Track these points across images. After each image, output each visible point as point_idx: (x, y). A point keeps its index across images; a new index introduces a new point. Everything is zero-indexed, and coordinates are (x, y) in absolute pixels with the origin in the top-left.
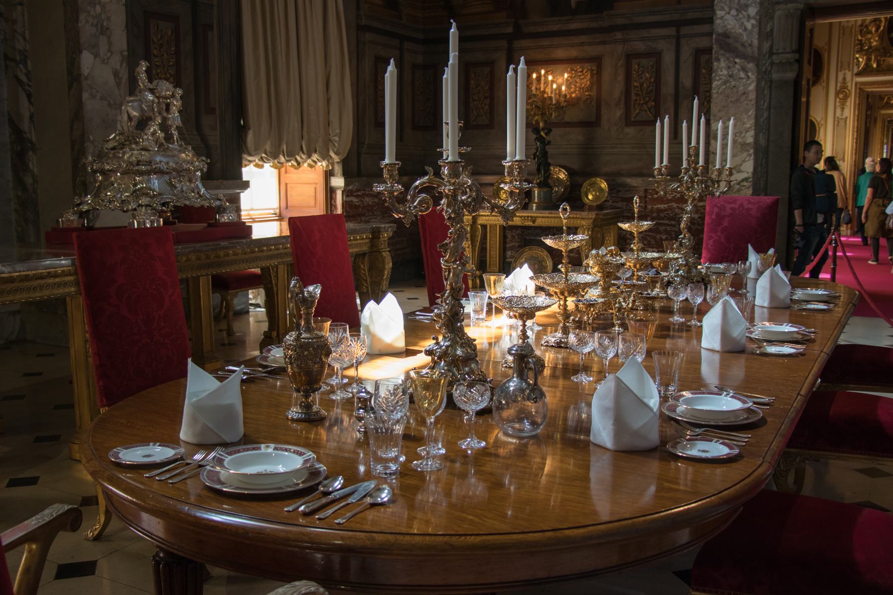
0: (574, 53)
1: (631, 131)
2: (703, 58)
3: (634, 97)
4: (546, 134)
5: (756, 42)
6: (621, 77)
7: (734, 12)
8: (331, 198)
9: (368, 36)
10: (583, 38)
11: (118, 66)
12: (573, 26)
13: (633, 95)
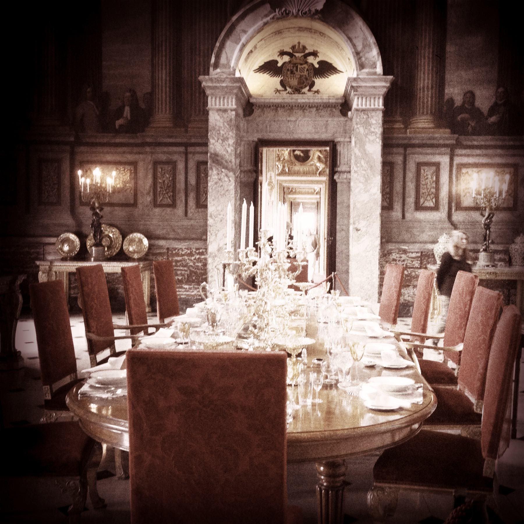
0: (118, 158)
1: (157, 210)
2: (202, 168)
3: (159, 190)
4: (100, 211)
5: (233, 160)
6: (150, 176)
7: (220, 141)
10: (125, 149)
12: (118, 140)
13: (158, 188)
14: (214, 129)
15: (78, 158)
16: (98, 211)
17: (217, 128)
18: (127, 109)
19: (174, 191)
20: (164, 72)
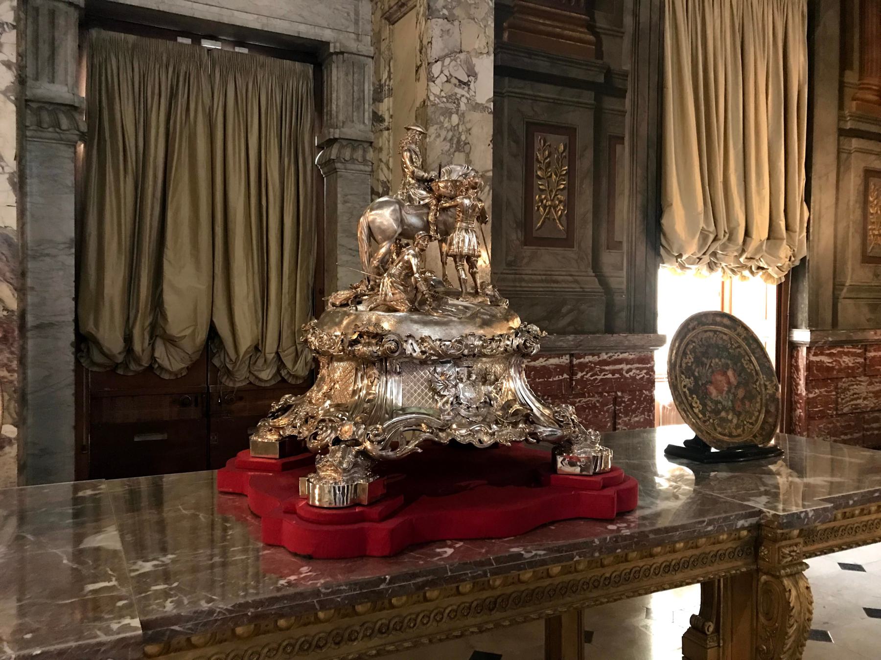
9: (855, 143)
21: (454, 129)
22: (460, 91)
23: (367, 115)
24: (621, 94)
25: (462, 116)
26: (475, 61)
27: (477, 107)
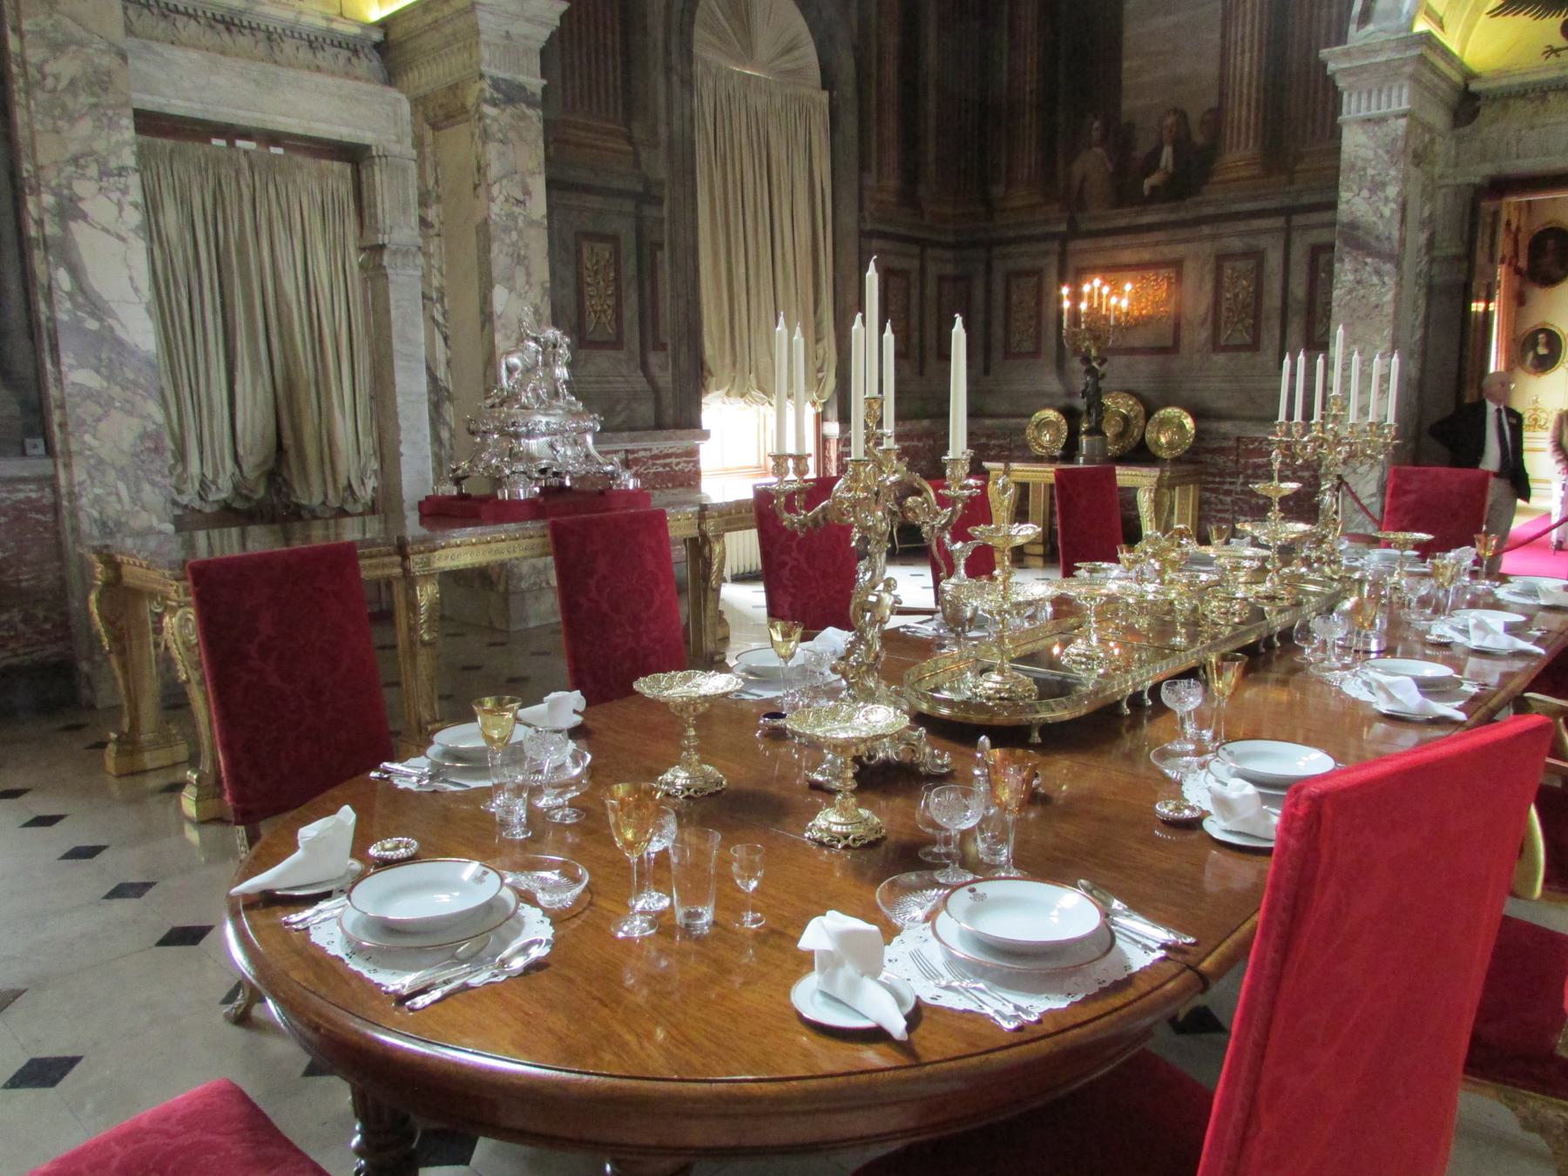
0: (1146, 255)
1: (1220, 358)
3: (1224, 313)
5: (1396, 234)
6: (1208, 287)
7: (1365, 193)
8: (825, 448)
10: (1159, 236)
11: (538, 301)
12: (1146, 219)
14: (1352, 167)
15: (1072, 263)
16: (1095, 364)
17: (1359, 164)
18: (1167, 151)
19: (1257, 317)
20: (1247, 55)
21: (513, 244)
22: (517, 210)
23: (414, 220)
24: (659, 201)
25: (520, 233)
26: (529, 180)
27: (531, 223)
